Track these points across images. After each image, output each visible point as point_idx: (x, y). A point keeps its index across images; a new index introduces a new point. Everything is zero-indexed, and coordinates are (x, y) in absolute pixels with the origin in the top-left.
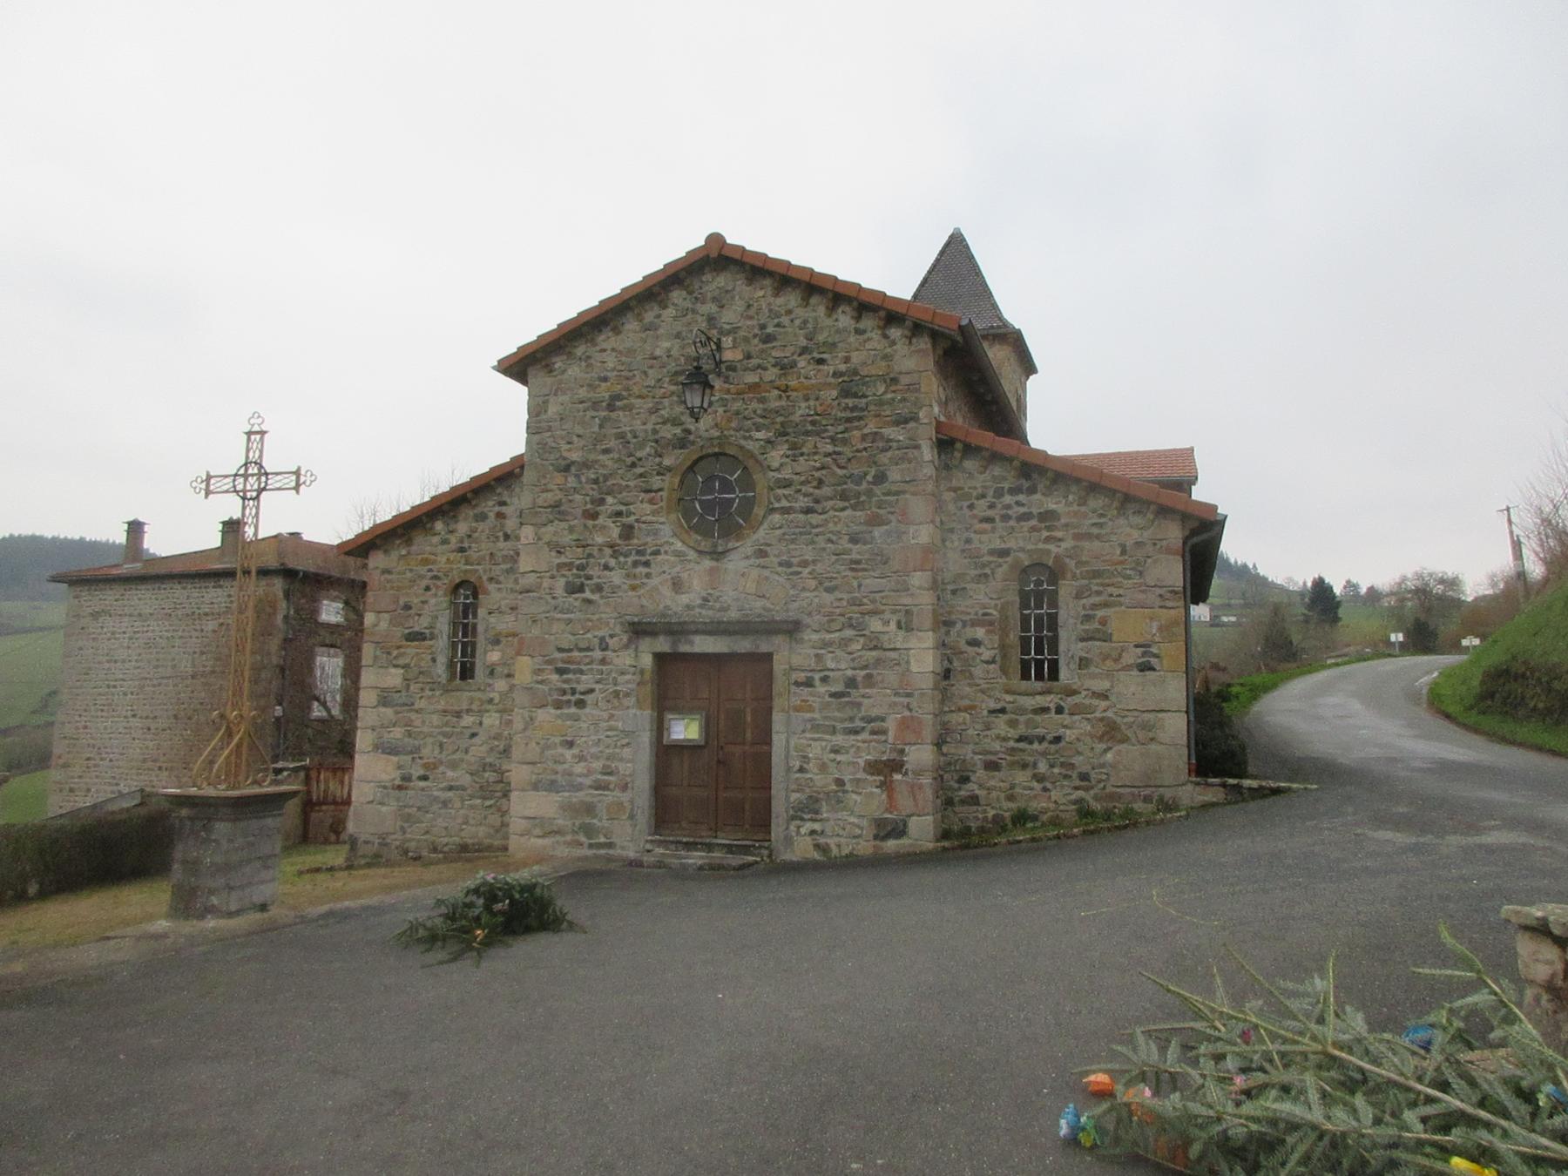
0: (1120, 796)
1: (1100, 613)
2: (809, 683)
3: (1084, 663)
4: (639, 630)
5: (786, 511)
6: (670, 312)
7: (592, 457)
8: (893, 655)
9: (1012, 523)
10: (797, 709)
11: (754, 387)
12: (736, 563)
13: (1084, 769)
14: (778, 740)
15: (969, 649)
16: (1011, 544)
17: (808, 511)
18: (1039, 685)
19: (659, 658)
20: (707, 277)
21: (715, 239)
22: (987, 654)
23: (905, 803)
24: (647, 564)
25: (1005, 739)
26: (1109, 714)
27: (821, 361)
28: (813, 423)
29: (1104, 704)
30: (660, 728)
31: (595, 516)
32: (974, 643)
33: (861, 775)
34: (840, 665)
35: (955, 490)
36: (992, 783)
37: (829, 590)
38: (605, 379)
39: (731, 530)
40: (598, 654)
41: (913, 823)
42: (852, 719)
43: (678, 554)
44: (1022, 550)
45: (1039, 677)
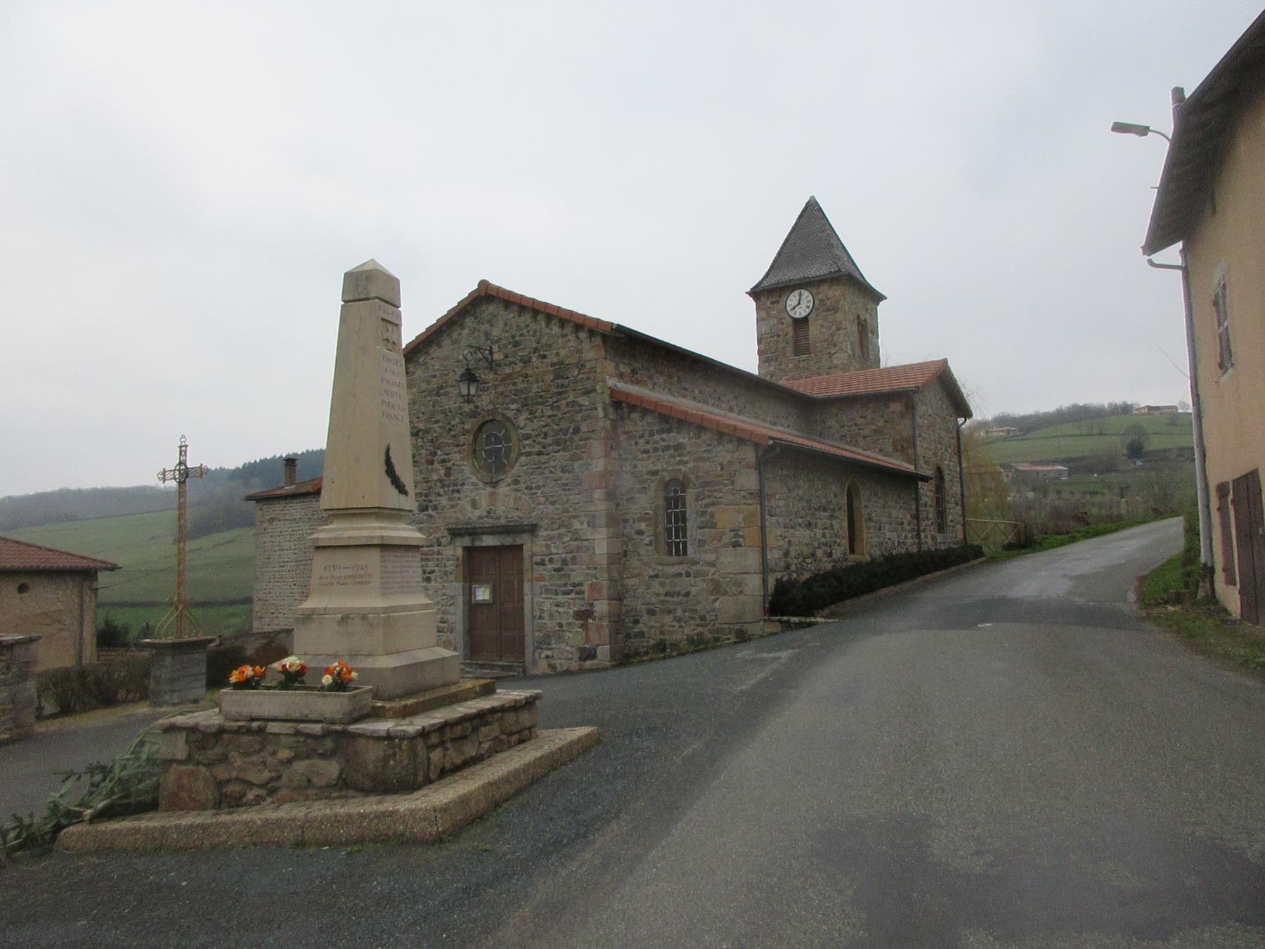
0: (722, 629)
1: (709, 510)
2: (542, 563)
3: (701, 543)
4: (455, 533)
5: (528, 454)
6: (466, 331)
7: (430, 426)
8: (585, 543)
9: (660, 453)
10: (537, 580)
11: (509, 376)
12: (503, 489)
13: (703, 613)
14: (527, 599)
15: (636, 536)
16: (659, 467)
17: (540, 453)
18: (674, 558)
19: (466, 549)
20: (484, 307)
21: (484, 284)
22: (647, 540)
23: (595, 638)
24: (458, 491)
25: (658, 595)
26: (716, 576)
27: (544, 357)
28: (541, 397)
29: (713, 570)
30: (469, 593)
31: (432, 463)
32: (640, 533)
33: (571, 620)
34: (558, 550)
35: (627, 433)
36: (652, 623)
37: (553, 503)
38: (434, 377)
39: (501, 469)
40: (436, 549)
41: (599, 649)
42: (566, 585)
43: (473, 484)
44: (665, 470)
45: (677, 553)
